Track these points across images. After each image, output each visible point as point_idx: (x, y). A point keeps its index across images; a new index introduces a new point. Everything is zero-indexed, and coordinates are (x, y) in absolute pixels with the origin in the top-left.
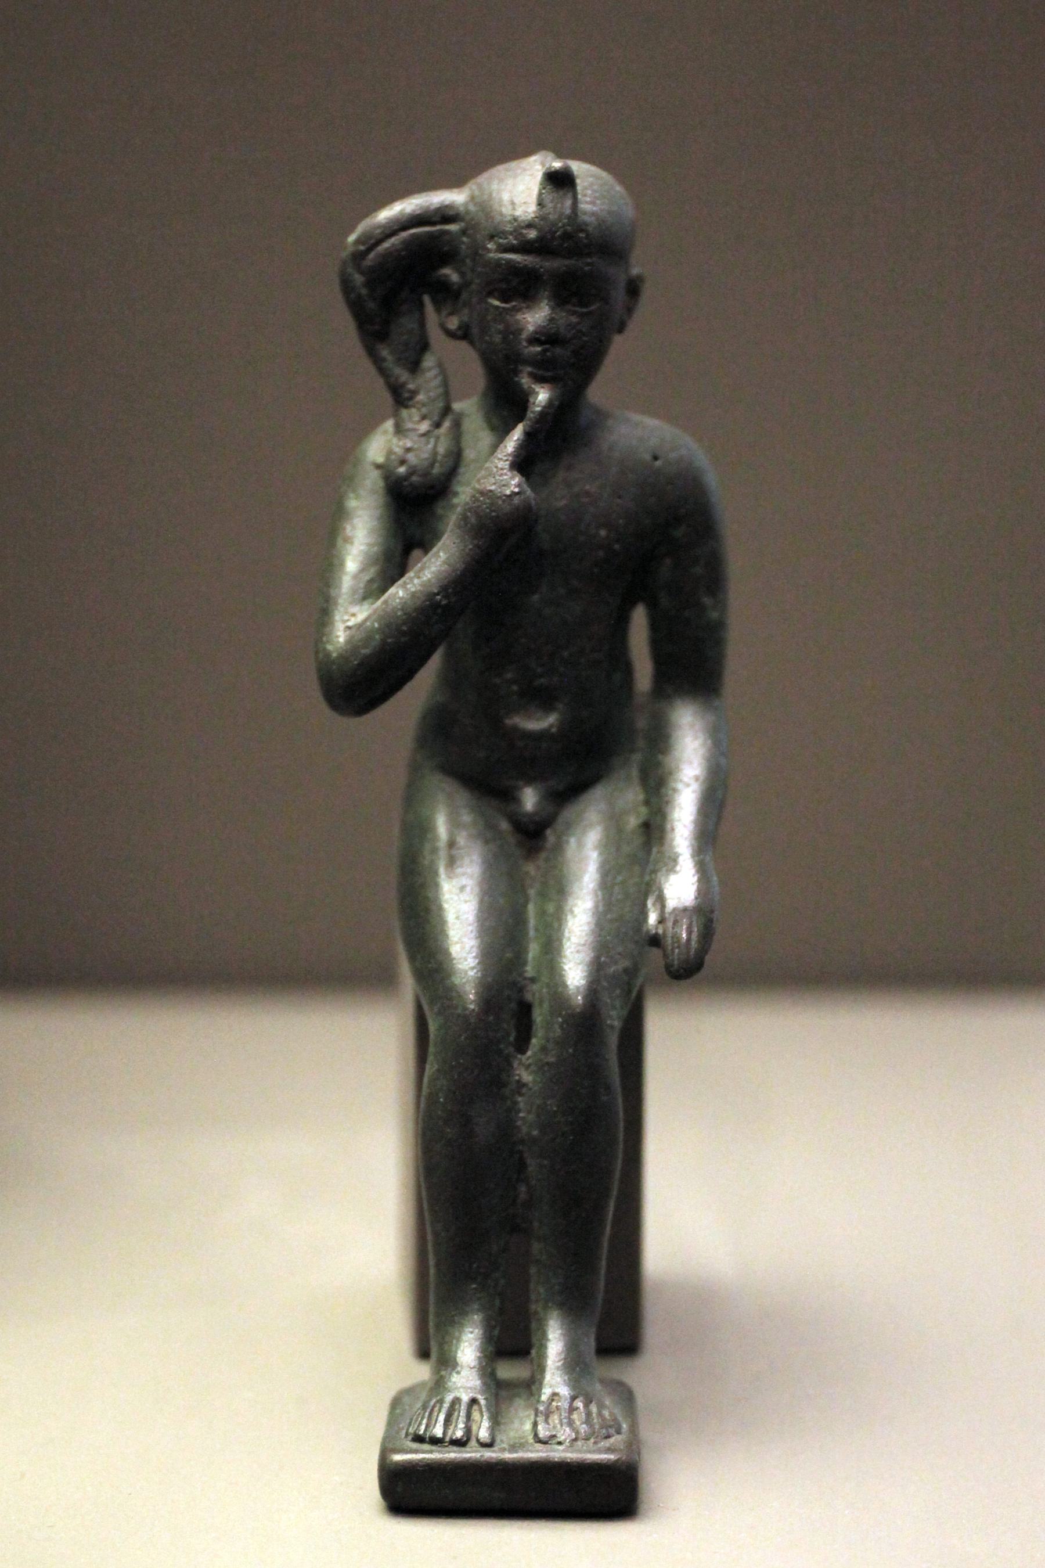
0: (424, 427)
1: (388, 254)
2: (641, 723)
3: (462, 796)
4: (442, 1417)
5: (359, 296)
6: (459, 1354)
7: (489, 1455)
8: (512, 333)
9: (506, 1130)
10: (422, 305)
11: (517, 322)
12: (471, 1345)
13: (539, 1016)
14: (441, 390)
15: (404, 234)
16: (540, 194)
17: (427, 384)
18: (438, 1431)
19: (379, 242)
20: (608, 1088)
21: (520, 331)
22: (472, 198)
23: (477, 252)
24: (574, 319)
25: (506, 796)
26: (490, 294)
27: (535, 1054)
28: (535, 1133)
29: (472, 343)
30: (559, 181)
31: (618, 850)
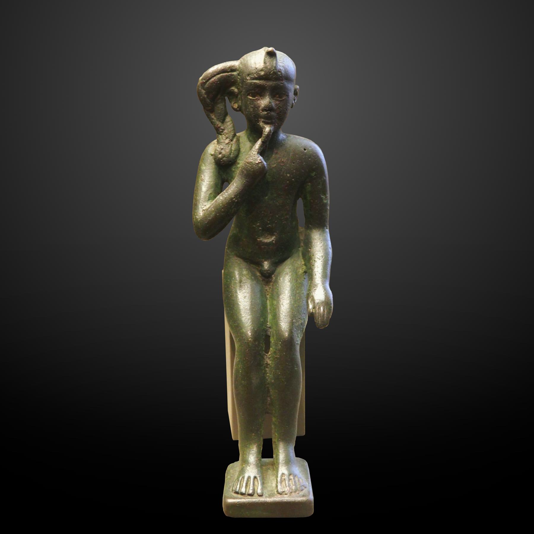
0: (227, 141)
1: (214, 82)
2: (302, 238)
3: (243, 264)
4: (244, 485)
5: (204, 97)
6: (250, 459)
7: (262, 499)
8: (257, 107)
9: (263, 379)
10: (225, 100)
11: (258, 104)
12: (253, 455)
13: (272, 340)
14: (232, 129)
15: (219, 76)
16: (265, 59)
17: (228, 125)
18: (243, 490)
19: (210, 79)
20: (297, 365)
21: (259, 107)
22: (241, 63)
23: (243, 81)
24: (277, 102)
25: (259, 264)
26: (248, 95)
27: (271, 354)
28: (273, 381)
29: (242, 112)
30: (271, 55)
31: (297, 280)
